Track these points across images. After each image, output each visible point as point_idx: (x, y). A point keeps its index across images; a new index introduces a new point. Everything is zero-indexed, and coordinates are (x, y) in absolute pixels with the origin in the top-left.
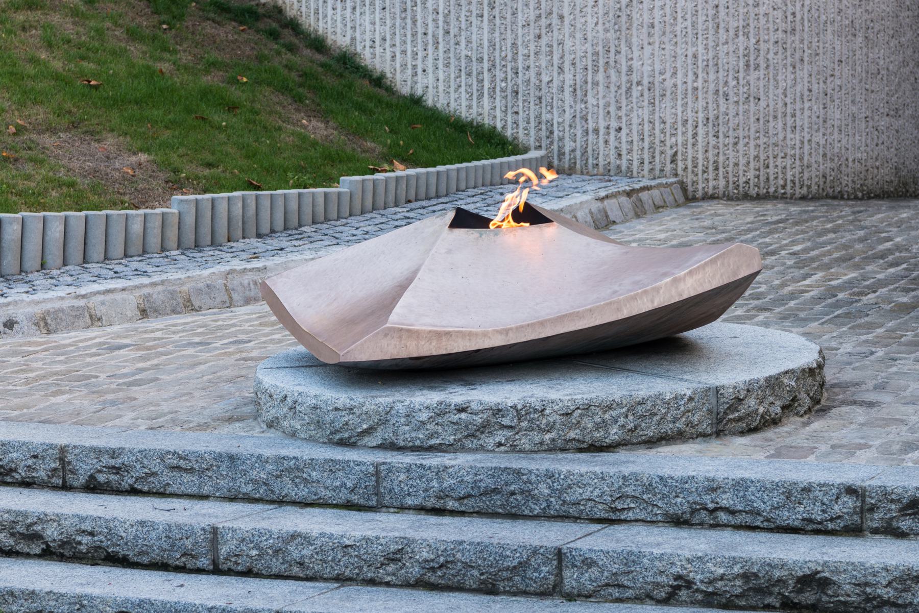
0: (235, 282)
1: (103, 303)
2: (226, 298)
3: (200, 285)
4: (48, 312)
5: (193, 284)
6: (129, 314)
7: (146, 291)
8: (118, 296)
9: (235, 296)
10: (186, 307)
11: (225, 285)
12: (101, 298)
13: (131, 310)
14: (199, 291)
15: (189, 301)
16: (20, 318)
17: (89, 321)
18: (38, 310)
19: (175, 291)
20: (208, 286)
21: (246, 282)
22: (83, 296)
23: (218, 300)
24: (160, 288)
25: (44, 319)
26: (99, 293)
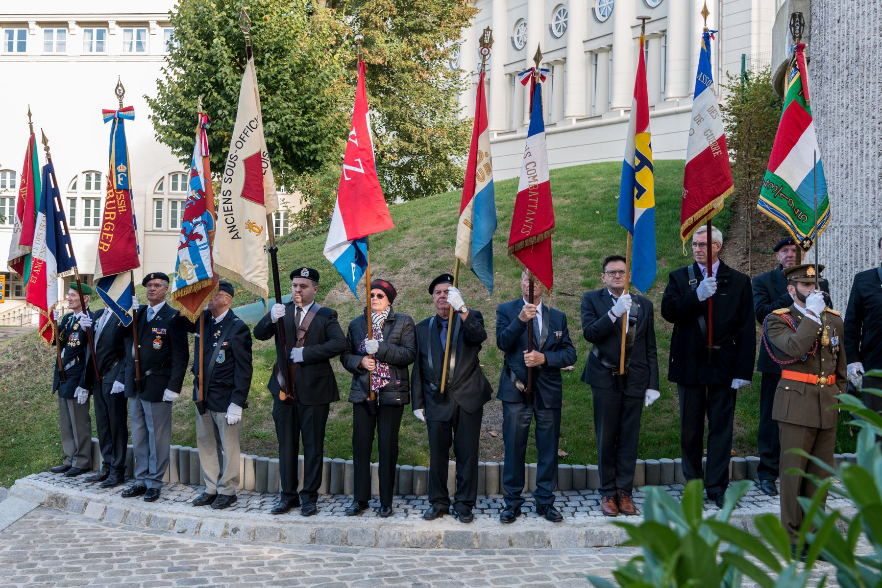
0: (385, 531)
1: (291, 529)
2: (374, 540)
3: (358, 529)
4: (258, 528)
5: (353, 528)
6: (304, 539)
7: (320, 526)
8: (302, 526)
9: (381, 541)
10: (342, 541)
11: (376, 532)
12: (291, 525)
13: (306, 537)
14: (355, 533)
15: (346, 538)
16: (242, 528)
17: (278, 538)
18: (253, 525)
19: (339, 530)
20: (363, 531)
21: (393, 532)
22: (282, 522)
23: (366, 541)
24: (330, 526)
25: (254, 531)
26: (290, 522)
